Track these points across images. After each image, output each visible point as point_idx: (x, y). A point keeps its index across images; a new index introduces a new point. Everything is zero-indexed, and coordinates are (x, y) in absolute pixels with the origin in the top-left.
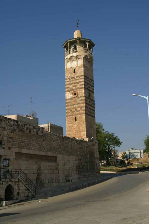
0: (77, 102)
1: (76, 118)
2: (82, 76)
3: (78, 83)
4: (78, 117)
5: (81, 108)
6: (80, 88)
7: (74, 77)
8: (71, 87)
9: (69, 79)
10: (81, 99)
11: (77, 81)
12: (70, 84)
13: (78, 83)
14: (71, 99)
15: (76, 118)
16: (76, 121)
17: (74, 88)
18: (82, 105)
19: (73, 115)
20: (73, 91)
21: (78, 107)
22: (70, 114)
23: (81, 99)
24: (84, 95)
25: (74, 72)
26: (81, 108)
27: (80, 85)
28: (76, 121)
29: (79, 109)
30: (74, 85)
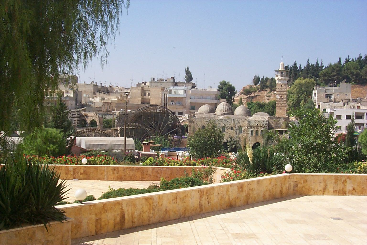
0: (282, 101)
1: (281, 108)
2: (285, 89)
3: (283, 92)
4: (282, 108)
5: (284, 104)
6: (284, 95)
7: (281, 89)
8: (279, 93)
9: (279, 89)
10: (284, 100)
11: (283, 91)
12: (280, 92)
13: (283, 92)
14: (279, 99)
15: (281, 108)
16: (281, 109)
17: (281, 94)
18: (285, 103)
19: (279, 107)
20: (280, 95)
21: (283, 103)
22: (278, 106)
23: (284, 100)
24: (286, 98)
25: (282, 86)
26: (284, 104)
27: (284, 93)
28: (281, 109)
29: (283, 104)
30: (281, 92)
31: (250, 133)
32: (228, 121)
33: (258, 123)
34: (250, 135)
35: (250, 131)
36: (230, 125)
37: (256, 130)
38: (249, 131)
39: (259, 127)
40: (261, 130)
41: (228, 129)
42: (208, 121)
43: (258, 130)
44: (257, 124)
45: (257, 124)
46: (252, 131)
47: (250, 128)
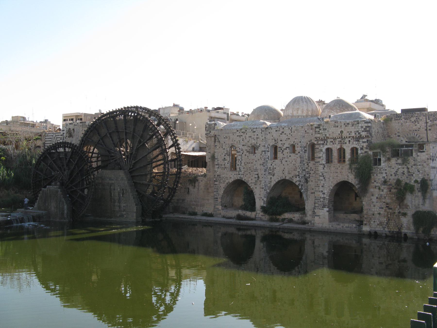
31: (324, 156)
32: (283, 132)
33: (343, 130)
34: (324, 162)
35: (324, 150)
36: (288, 142)
37: (339, 147)
38: (321, 150)
39: (347, 141)
40: (353, 146)
41: (283, 151)
42: (242, 134)
43: (344, 146)
44: (342, 132)
45: (342, 132)
46: (329, 151)
47: (323, 144)
